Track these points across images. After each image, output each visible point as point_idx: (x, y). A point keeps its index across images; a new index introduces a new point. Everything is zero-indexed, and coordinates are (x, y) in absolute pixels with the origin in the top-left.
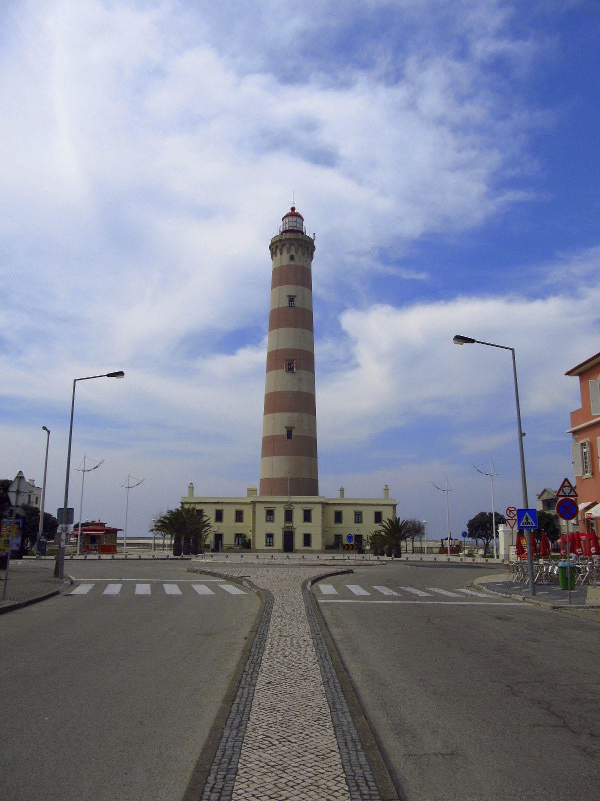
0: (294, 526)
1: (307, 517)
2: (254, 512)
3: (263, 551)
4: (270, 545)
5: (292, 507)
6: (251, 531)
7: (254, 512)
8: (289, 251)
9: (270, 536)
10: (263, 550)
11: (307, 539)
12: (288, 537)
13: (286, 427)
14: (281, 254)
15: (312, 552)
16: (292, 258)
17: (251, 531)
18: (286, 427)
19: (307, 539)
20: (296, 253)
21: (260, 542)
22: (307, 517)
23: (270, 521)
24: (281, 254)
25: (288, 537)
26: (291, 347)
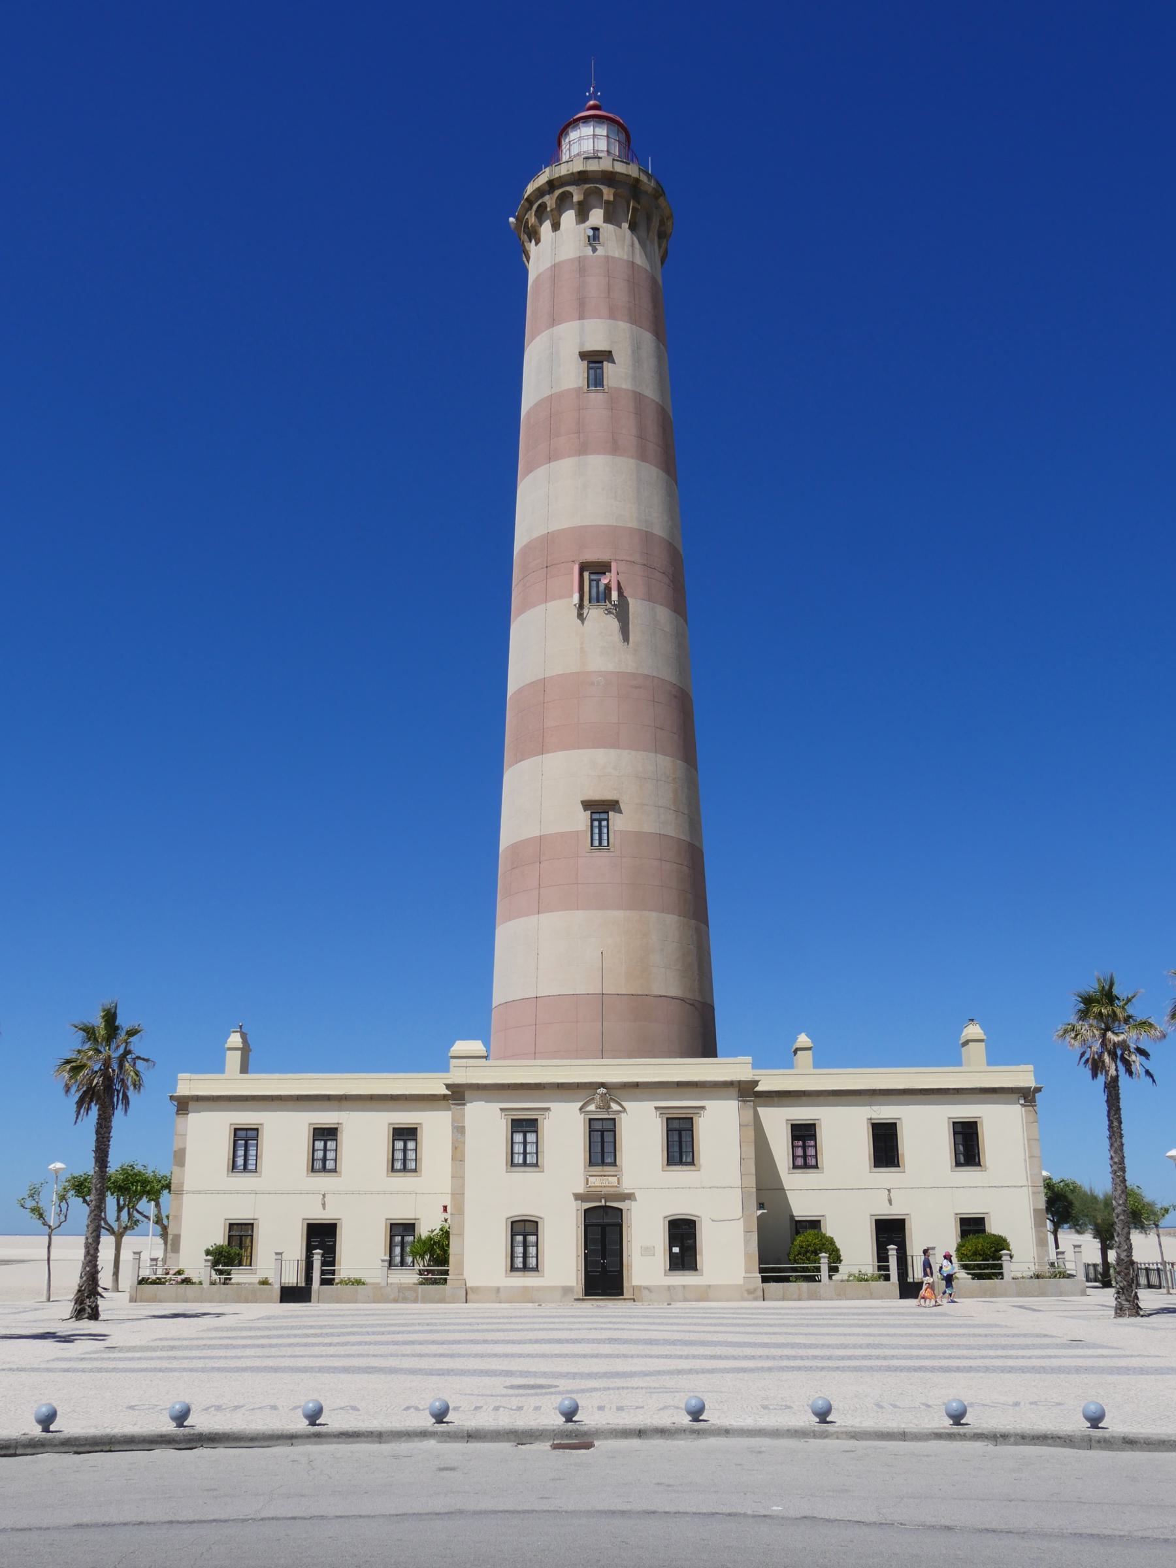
0: (627, 1187)
1: (680, 1144)
2: (459, 1130)
3: (497, 1294)
4: (525, 1268)
5: (615, 1107)
6: (445, 1208)
7: (459, 1130)
8: (582, 216)
9: (524, 1230)
10: (498, 1289)
11: (683, 1239)
12: (603, 1232)
13: (587, 805)
14: (556, 226)
15: (704, 1294)
16: (595, 237)
17: (445, 1208)
18: (587, 805)
19: (683, 1239)
20: (608, 219)
21: (481, 1256)
22: (680, 1144)
23: (525, 1164)
24: (556, 226)
25: (603, 1232)
26: (600, 522)
